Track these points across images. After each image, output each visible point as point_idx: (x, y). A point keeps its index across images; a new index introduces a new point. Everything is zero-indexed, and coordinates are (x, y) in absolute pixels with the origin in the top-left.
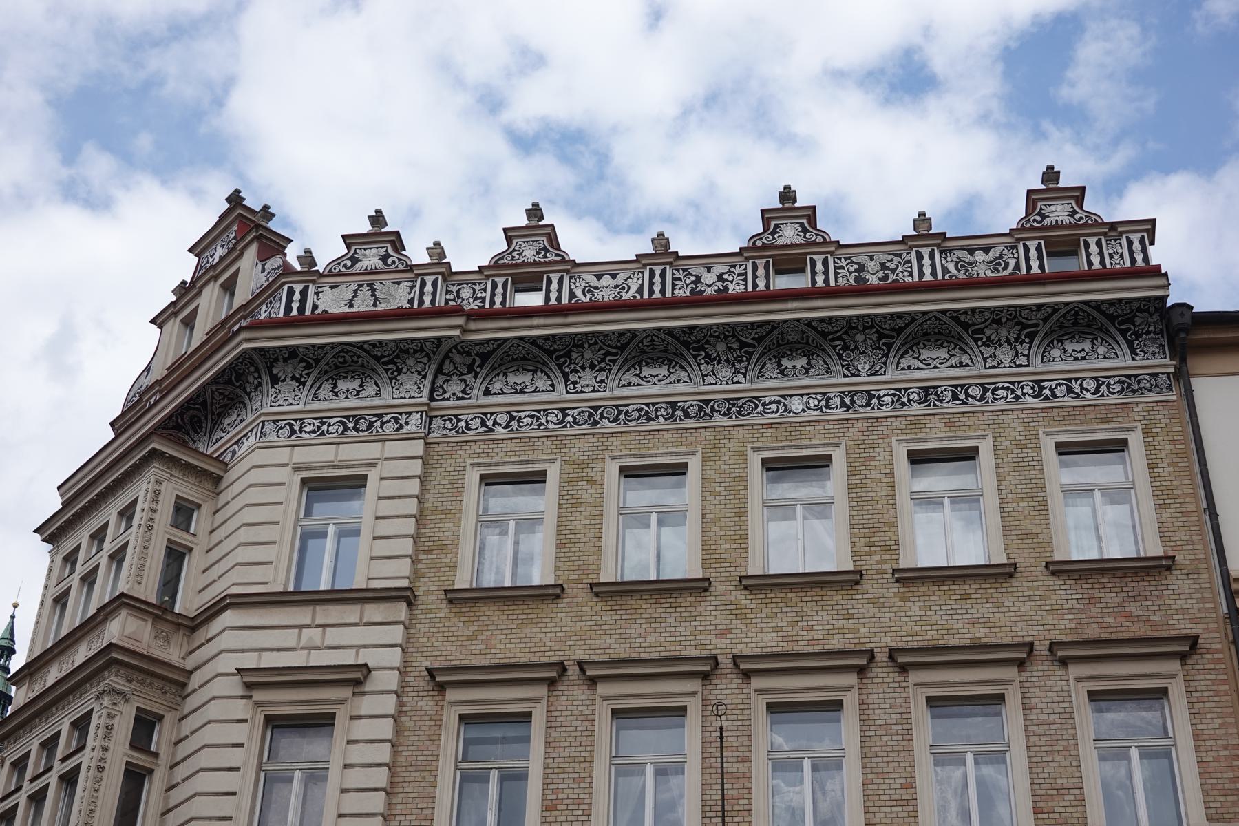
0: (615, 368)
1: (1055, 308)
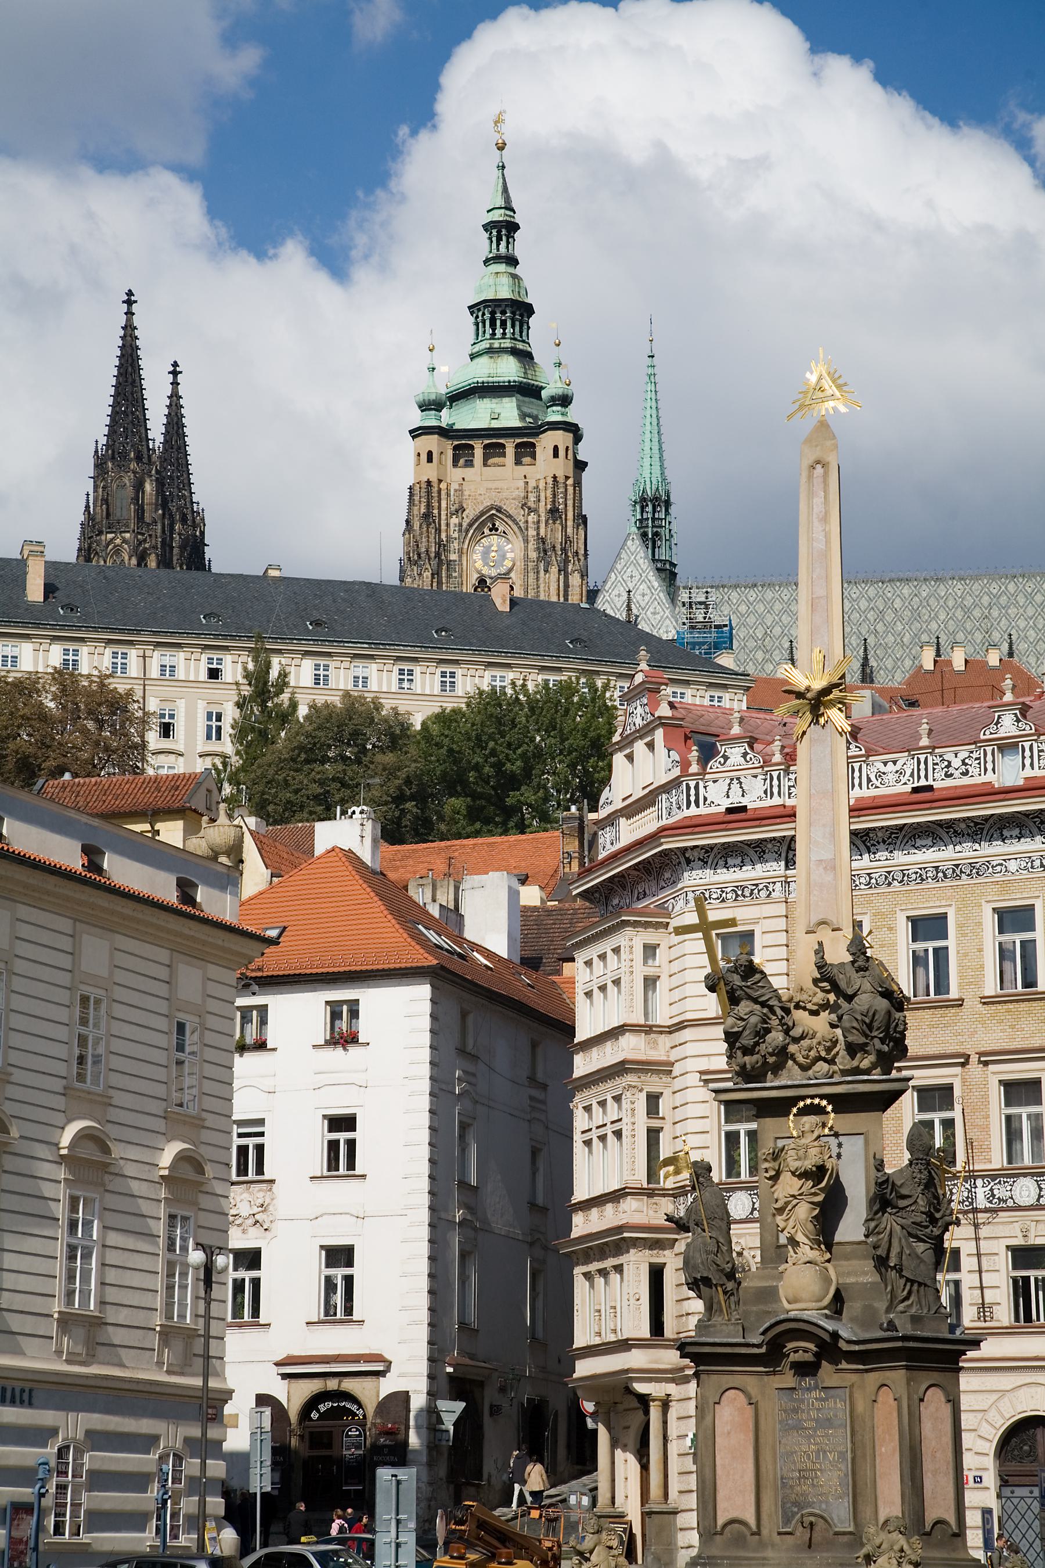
0: (899, 842)
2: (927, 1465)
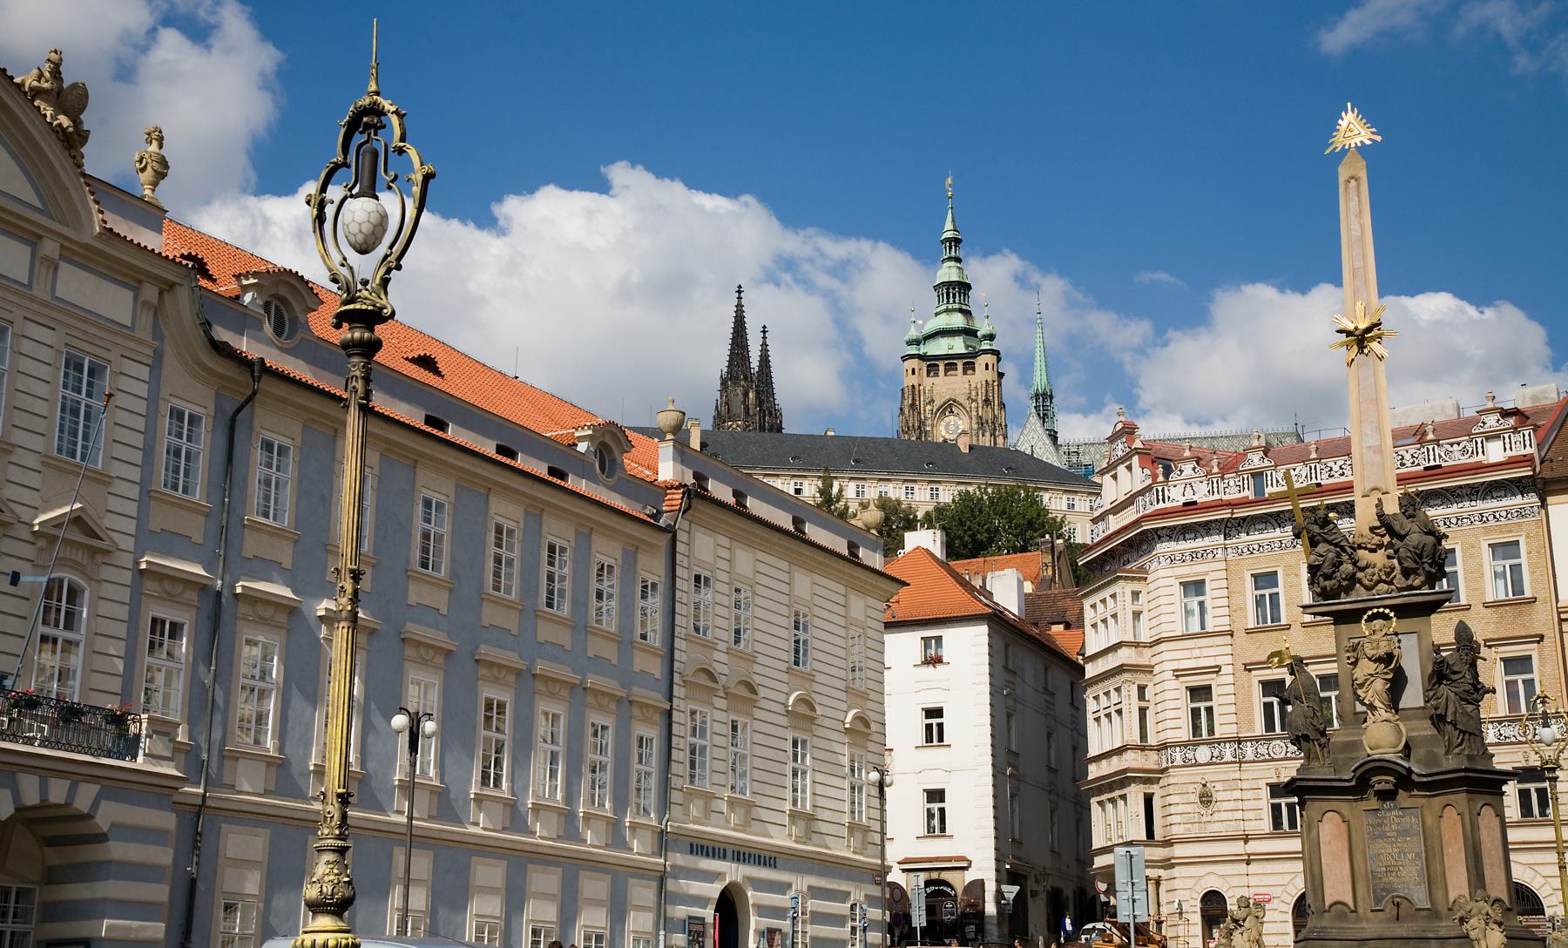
2: (1486, 860)
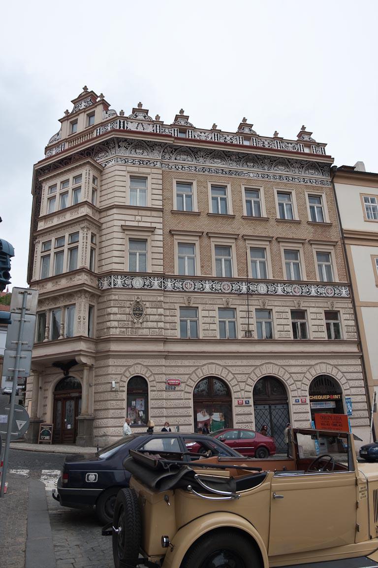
1: (309, 162)
